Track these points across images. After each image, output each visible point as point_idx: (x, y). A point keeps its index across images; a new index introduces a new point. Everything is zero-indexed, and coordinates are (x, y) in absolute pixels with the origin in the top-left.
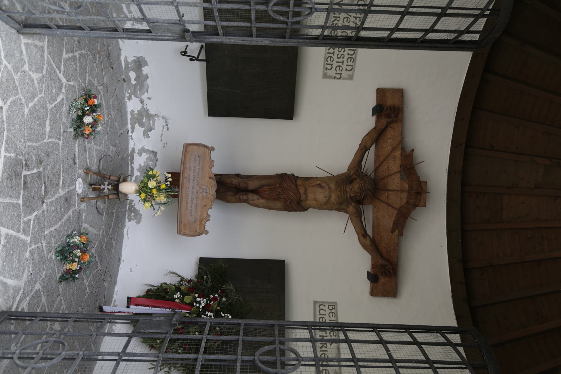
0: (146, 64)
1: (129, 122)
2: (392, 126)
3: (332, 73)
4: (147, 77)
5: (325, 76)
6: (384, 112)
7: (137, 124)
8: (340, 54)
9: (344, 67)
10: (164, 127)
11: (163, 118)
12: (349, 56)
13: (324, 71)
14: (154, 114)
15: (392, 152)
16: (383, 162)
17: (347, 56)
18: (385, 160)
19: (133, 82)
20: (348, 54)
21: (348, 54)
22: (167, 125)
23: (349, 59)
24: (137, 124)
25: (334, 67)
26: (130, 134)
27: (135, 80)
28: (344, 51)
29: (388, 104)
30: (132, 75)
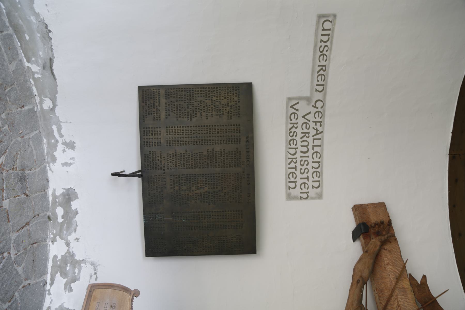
0: (76, 197)
1: (49, 271)
2: (386, 247)
3: (297, 192)
4: (77, 213)
5: (289, 197)
6: (372, 231)
7: (59, 274)
8: (304, 168)
9: (310, 183)
10: (91, 276)
11: (92, 264)
12: (314, 170)
13: (287, 191)
14: (81, 259)
15: (397, 282)
16: (388, 300)
17: (311, 171)
18: (391, 296)
19: (60, 220)
20: (313, 167)
21: (313, 167)
22: (95, 273)
23: (315, 174)
24: (59, 274)
25: (298, 184)
26: (48, 287)
27: (63, 217)
28: (307, 165)
29: (373, 221)
30: (60, 211)
